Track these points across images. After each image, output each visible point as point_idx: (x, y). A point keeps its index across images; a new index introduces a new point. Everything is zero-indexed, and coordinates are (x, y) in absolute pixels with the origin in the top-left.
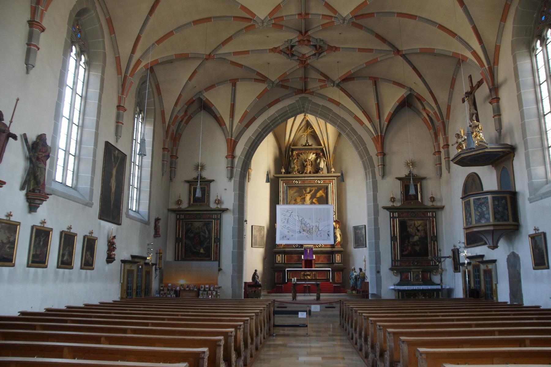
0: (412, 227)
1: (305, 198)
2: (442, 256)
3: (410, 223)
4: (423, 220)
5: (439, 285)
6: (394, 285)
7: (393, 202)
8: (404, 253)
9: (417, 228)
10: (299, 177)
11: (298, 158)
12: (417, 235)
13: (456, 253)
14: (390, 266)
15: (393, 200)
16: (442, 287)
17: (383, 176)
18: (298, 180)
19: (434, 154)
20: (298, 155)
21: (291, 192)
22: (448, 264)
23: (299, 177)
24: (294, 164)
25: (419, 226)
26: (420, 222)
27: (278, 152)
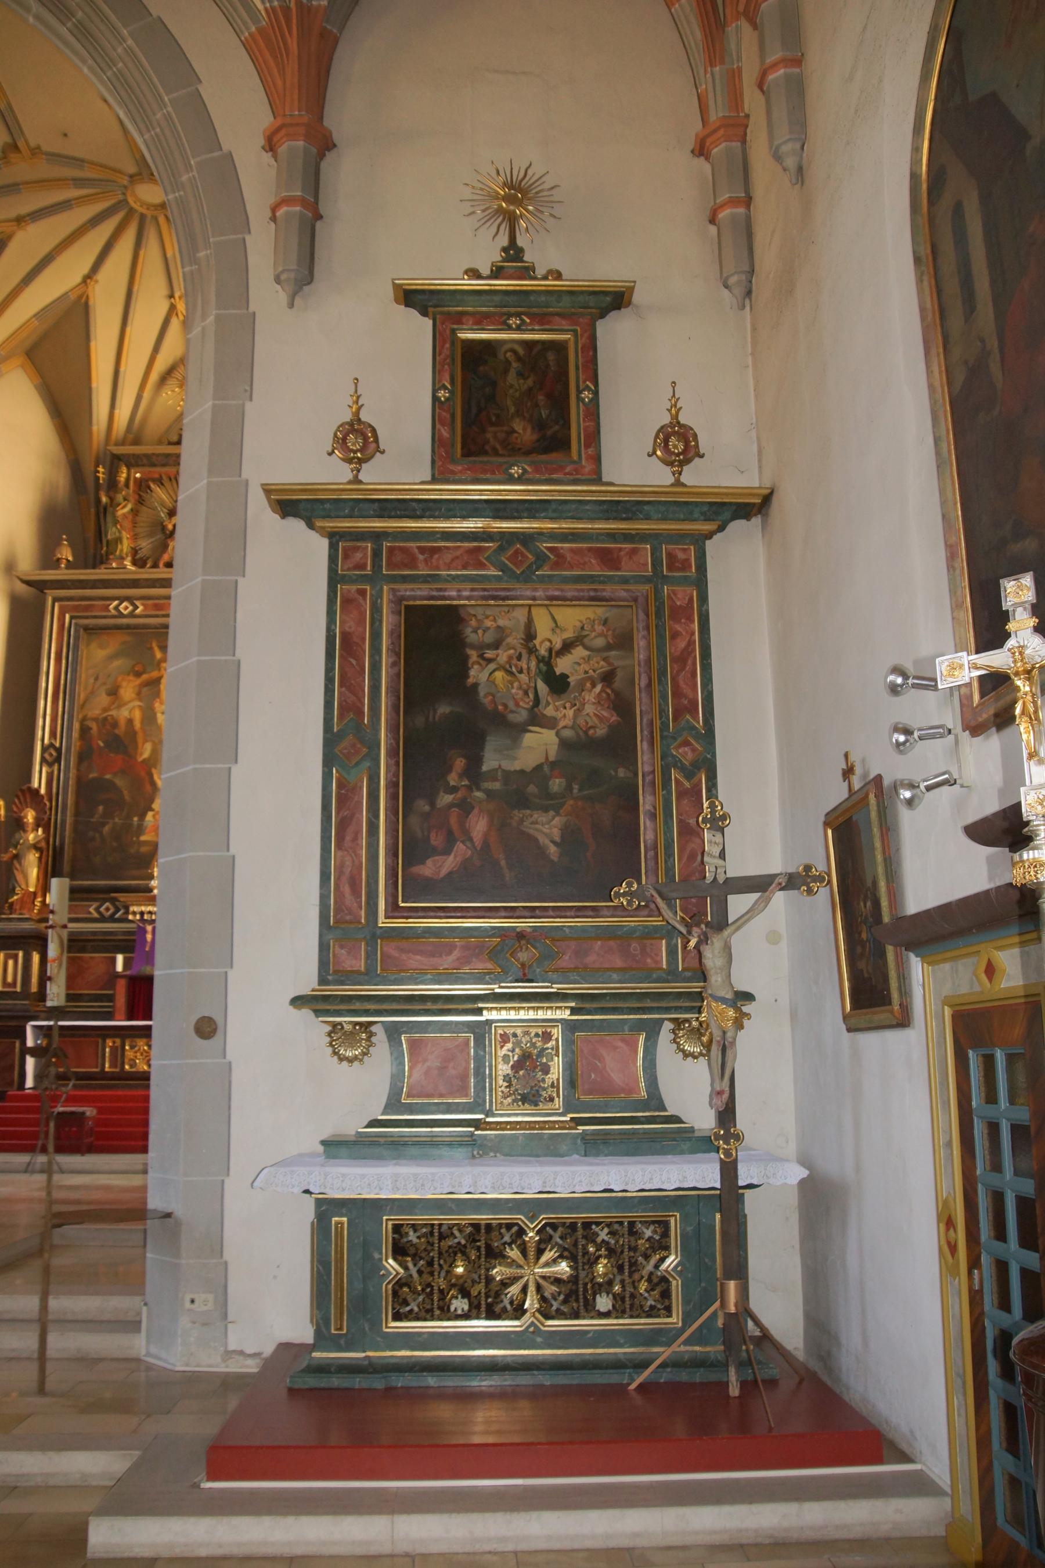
0: (503, 656)
1: (158, 681)
2: (737, 867)
3: (485, 621)
4: (597, 599)
5: (705, 1144)
6: (336, 1147)
7: (358, 460)
8: (428, 869)
9: (547, 663)
10: (135, 583)
11: (141, 501)
12: (550, 723)
13: (859, 834)
14: (308, 982)
15: (357, 439)
16: (729, 1170)
17: (303, 272)
18: (130, 599)
19: (701, 150)
20: (142, 486)
21: (97, 654)
22: (777, 954)
23: (135, 583)
24: (116, 522)
25: (567, 647)
26: (572, 618)
27: (62, 481)
